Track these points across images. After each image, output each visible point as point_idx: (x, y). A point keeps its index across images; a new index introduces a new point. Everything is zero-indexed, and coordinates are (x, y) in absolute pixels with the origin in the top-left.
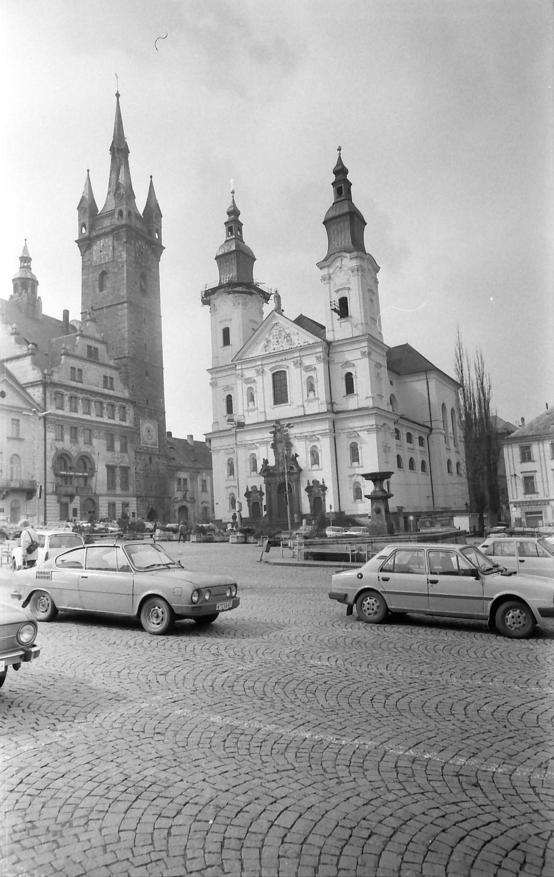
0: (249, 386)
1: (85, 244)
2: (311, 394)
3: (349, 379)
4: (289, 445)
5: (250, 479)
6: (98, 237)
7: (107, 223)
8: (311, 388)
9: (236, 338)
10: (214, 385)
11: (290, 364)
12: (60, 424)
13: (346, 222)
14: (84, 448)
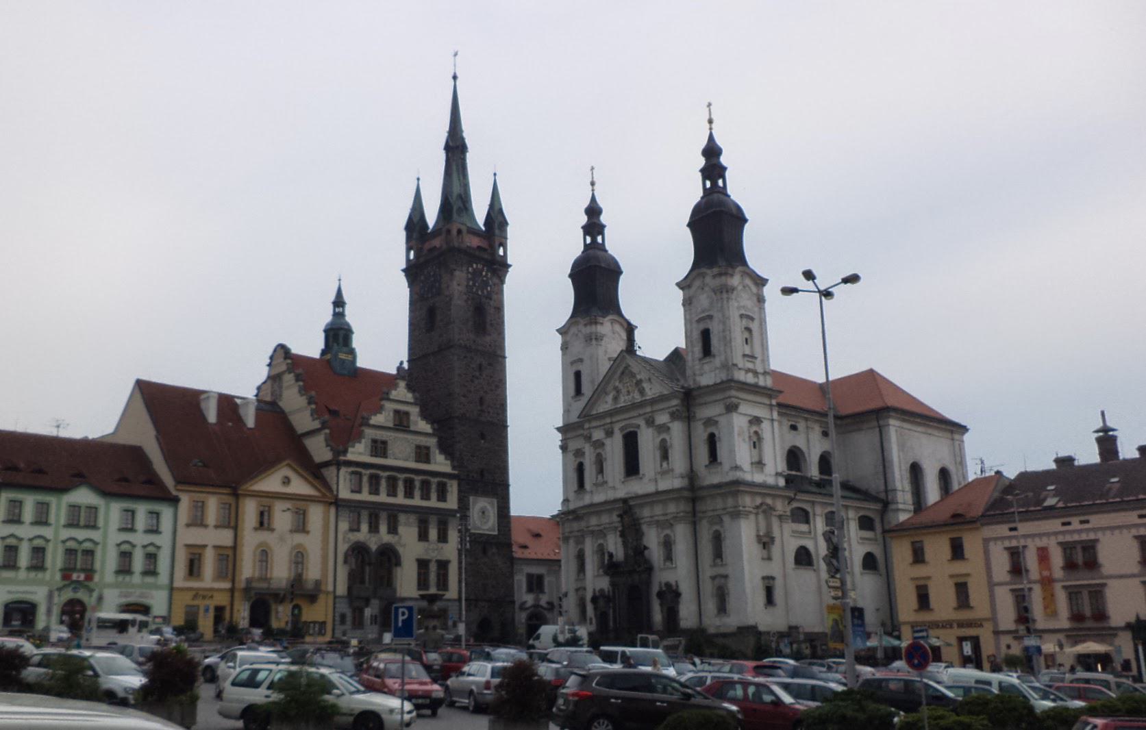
1: (412, 272)
2: (665, 465)
3: (712, 441)
4: (639, 534)
7: (437, 242)
10: (564, 448)
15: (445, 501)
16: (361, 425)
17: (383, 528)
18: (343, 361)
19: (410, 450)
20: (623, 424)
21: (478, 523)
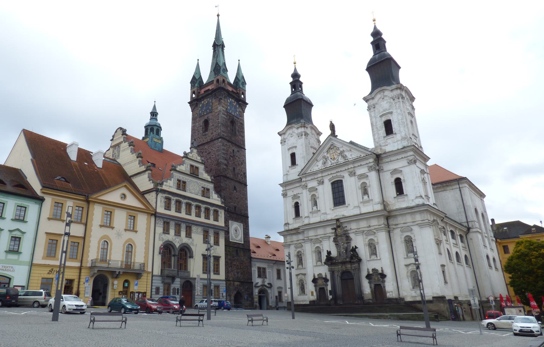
0: (312, 193)
1: (193, 103)
2: (366, 197)
5: (315, 268)
6: (203, 98)
8: (365, 192)
9: (301, 162)
11: (346, 175)
12: (167, 221)
13: (383, 70)
14: (185, 240)
15: (218, 221)
16: (171, 170)
17: (183, 233)
18: (156, 143)
19: (199, 189)
20: (331, 176)
21: (234, 237)
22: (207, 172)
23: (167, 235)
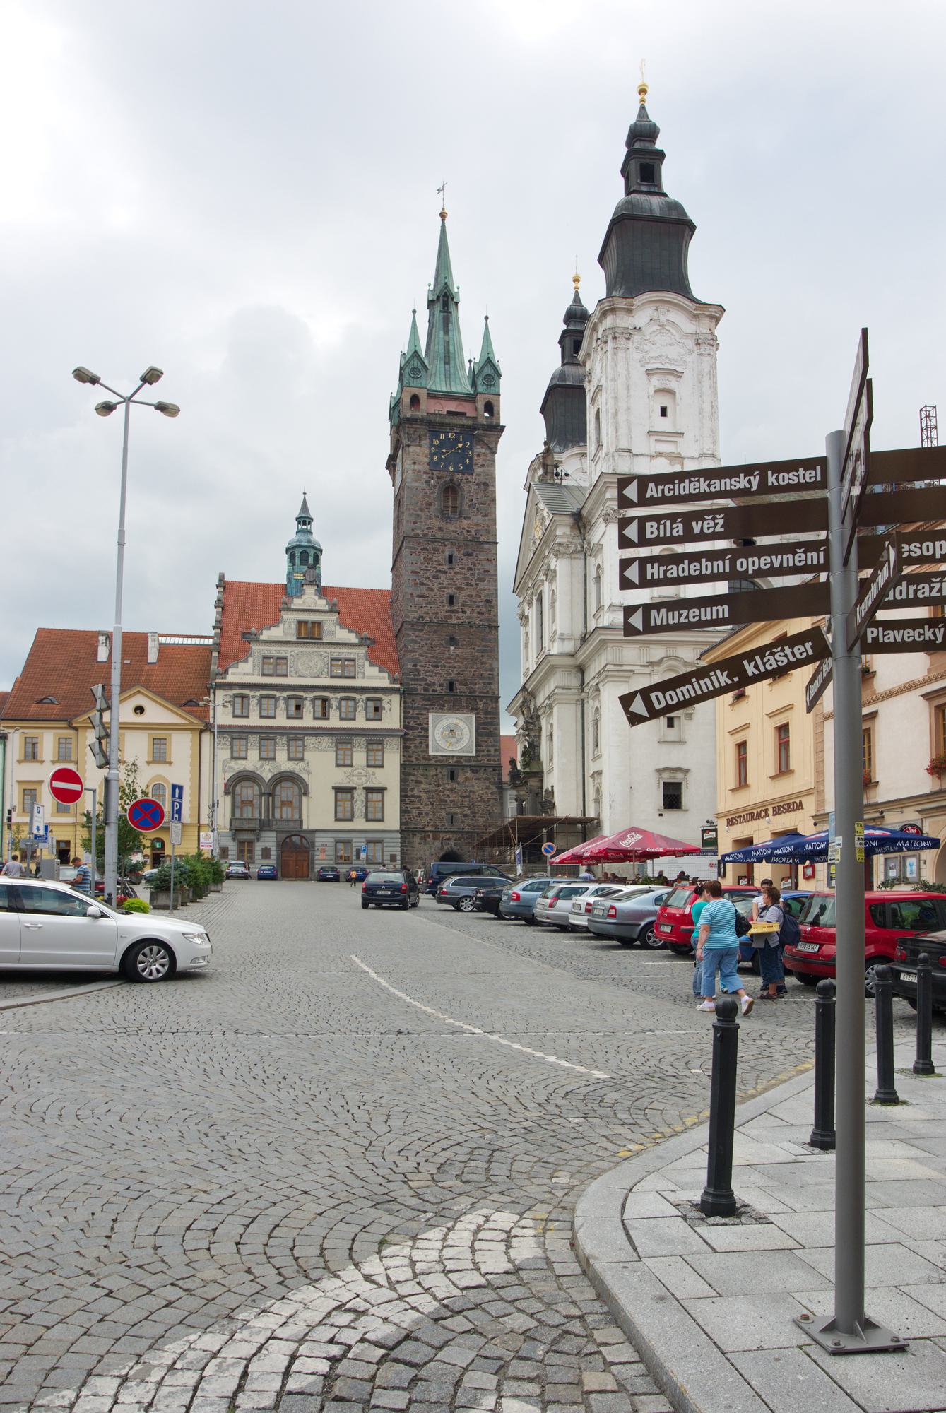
1: (391, 464)
17: (281, 755)
22: (343, 625)
23: (240, 762)
